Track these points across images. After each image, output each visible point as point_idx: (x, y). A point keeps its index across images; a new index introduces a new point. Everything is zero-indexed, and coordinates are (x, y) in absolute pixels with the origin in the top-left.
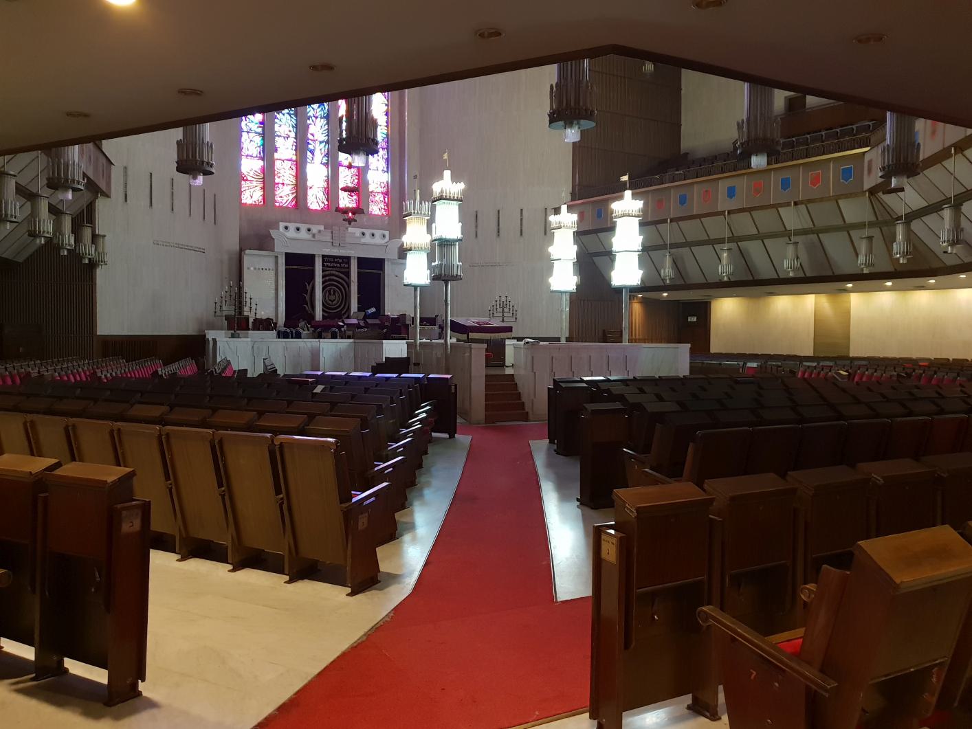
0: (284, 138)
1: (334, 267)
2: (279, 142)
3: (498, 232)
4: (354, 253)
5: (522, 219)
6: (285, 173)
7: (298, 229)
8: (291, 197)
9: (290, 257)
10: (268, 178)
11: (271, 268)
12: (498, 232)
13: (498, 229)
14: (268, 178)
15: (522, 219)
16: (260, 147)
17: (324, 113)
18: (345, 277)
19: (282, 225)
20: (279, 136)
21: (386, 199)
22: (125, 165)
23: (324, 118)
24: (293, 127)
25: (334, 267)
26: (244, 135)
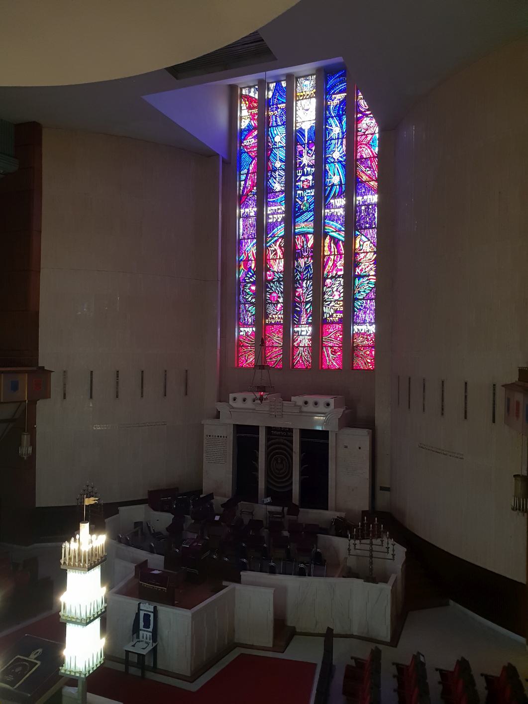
0: (274, 304)
1: (281, 435)
2: (271, 309)
3: (443, 409)
4: (297, 425)
5: (466, 397)
6: (276, 338)
7: (244, 400)
8: (279, 358)
9: (239, 429)
10: (261, 340)
11: (225, 436)
12: (443, 409)
13: (443, 406)
14: (261, 340)
15: (466, 397)
16: (253, 315)
17: (310, 275)
18: (289, 444)
19: (231, 396)
20: (269, 303)
21: (373, 352)
22: (64, 369)
23: (310, 279)
24: (281, 292)
25: (281, 435)
26: (242, 306)
